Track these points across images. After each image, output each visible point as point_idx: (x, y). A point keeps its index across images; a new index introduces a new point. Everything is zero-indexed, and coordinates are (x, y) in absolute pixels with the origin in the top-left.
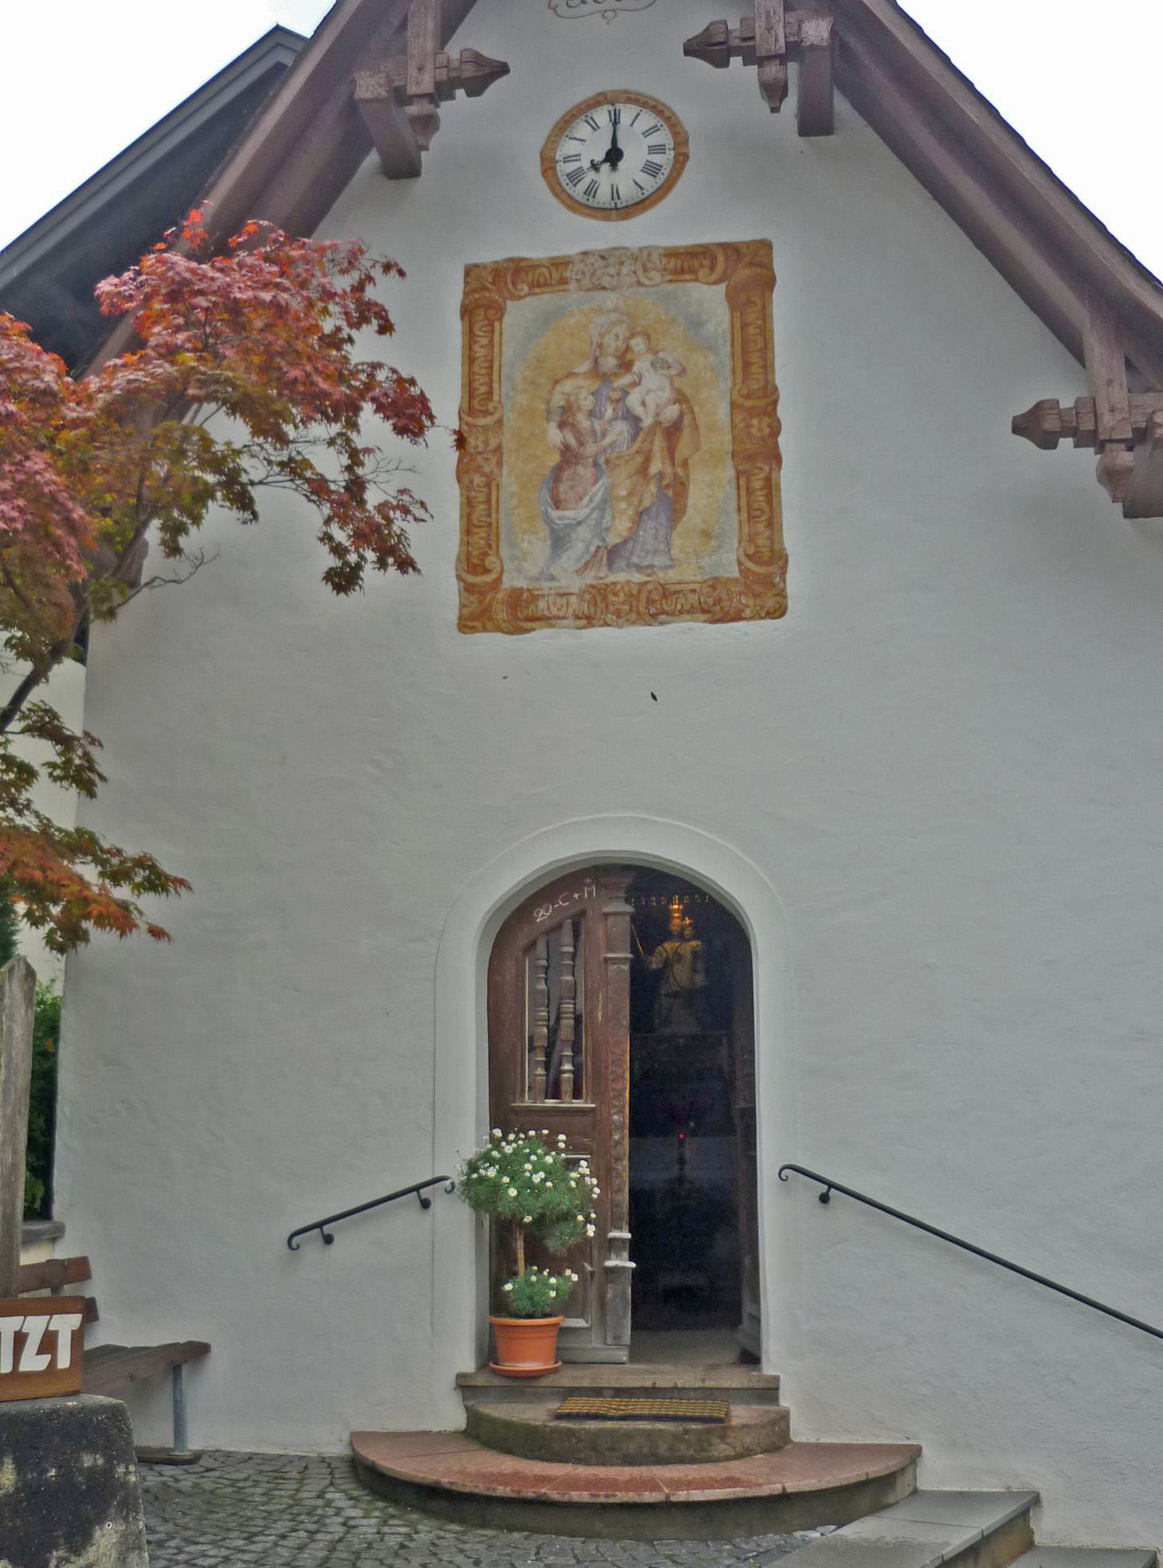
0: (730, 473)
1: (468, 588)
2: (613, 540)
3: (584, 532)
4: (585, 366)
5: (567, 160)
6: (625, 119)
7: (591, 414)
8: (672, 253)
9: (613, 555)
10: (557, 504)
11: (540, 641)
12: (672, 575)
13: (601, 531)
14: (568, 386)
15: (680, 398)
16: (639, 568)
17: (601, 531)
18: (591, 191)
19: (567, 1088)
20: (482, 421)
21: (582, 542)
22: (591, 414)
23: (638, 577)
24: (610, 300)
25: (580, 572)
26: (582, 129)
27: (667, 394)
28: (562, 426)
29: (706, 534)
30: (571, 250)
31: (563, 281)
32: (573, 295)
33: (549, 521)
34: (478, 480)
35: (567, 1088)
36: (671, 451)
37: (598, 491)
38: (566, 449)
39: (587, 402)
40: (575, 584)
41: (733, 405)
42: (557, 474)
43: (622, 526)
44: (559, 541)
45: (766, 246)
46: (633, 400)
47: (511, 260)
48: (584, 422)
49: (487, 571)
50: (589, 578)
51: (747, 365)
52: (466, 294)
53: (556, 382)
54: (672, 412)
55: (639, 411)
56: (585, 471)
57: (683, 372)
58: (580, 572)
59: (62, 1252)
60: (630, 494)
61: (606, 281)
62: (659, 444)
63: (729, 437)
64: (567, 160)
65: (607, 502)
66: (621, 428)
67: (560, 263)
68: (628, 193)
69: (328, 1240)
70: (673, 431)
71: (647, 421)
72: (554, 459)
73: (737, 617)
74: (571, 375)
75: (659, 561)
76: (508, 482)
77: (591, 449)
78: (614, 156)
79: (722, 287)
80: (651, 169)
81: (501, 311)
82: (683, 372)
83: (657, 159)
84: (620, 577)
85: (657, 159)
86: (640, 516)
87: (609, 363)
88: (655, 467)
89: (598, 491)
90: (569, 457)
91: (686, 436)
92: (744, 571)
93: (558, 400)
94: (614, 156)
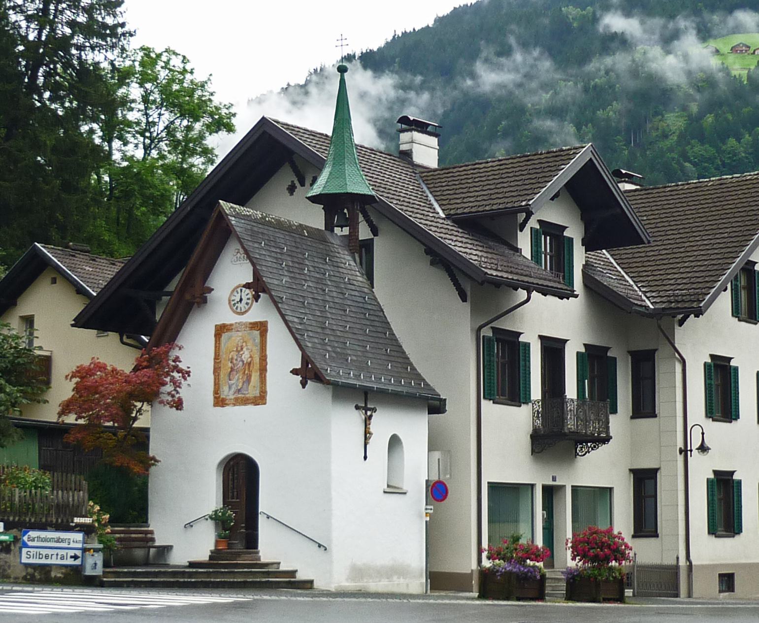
0: (258, 374)
1: (215, 398)
2: (239, 388)
3: (234, 386)
4: (235, 349)
5: (233, 301)
6: (243, 291)
7: (236, 360)
8: (251, 323)
9: (239, 390)
10: (230, 380)
11: (227, 408)
12: (247, 396)
13: (237, 386)
14: (232, 353)
15: (251, 357)
16: (243, 394)
17: (237, 386)
18: (237, 308)
19: (235, 497)
20: (218, 361)
21: (233, 390)
22: (236, 360)
23: (243, 396)
24: (240, 334)
25: (233, 394)
26: (235, 293)
27: (249, 356)
28: (231, 362)
29: (254, 387)
30: (233, 322)
31: (232, 329)
32: (233, 333)
33: (229, 383)
34: (217, 374)
35: (235, 497)
36: (249, 368)
37: (236, 377)
38: (232, 368)
39: (235, 357)
40: (233, 397)
41: (260, 359)
42: (230, 374)
43: (240, 385)
44: (230, 388)
45: (266, 322)
46: (243, 357)
47: (223, 324)
48: (235, 362)
49: (218, 394)
50: (235, 396)
51: (263, 349)
52: (216, 331)
53: (230, 352)
54: (249, 360)
55: (244, 359)
56: (235, 373)
57: (252, 351)
58: (233, 394)
59: (150, 529)
60: (242, 378)
61: (239, 330)
62: (247, 367)
63: (258, 366)
64: (233, 301)
65: (238, 379)
66: (241, 363)
67: (231, 325)
68: (243, 310)
69: (192, 526)
70: (249, 364)
71: (245, 362)
72: (229, 370)
73: (259, 405)
74: (233, 351)
75: (247, 392)
76: (222, 376)
77: (236, 368)
78: (241, 300)
79: (259, 332)
80: (247, 304)
81: (221, 336)
82: (252, 351)
83: (248, 301)
84: (240, 396)
85: (248, 301)
86: (244, 382)
87: (239, 349)
88: (246, 372)
89: (236, 377)
90: (232, 369)
91: (252, 365)
92: (260, 394)
93: (230, 357)
94: (241, 300)
